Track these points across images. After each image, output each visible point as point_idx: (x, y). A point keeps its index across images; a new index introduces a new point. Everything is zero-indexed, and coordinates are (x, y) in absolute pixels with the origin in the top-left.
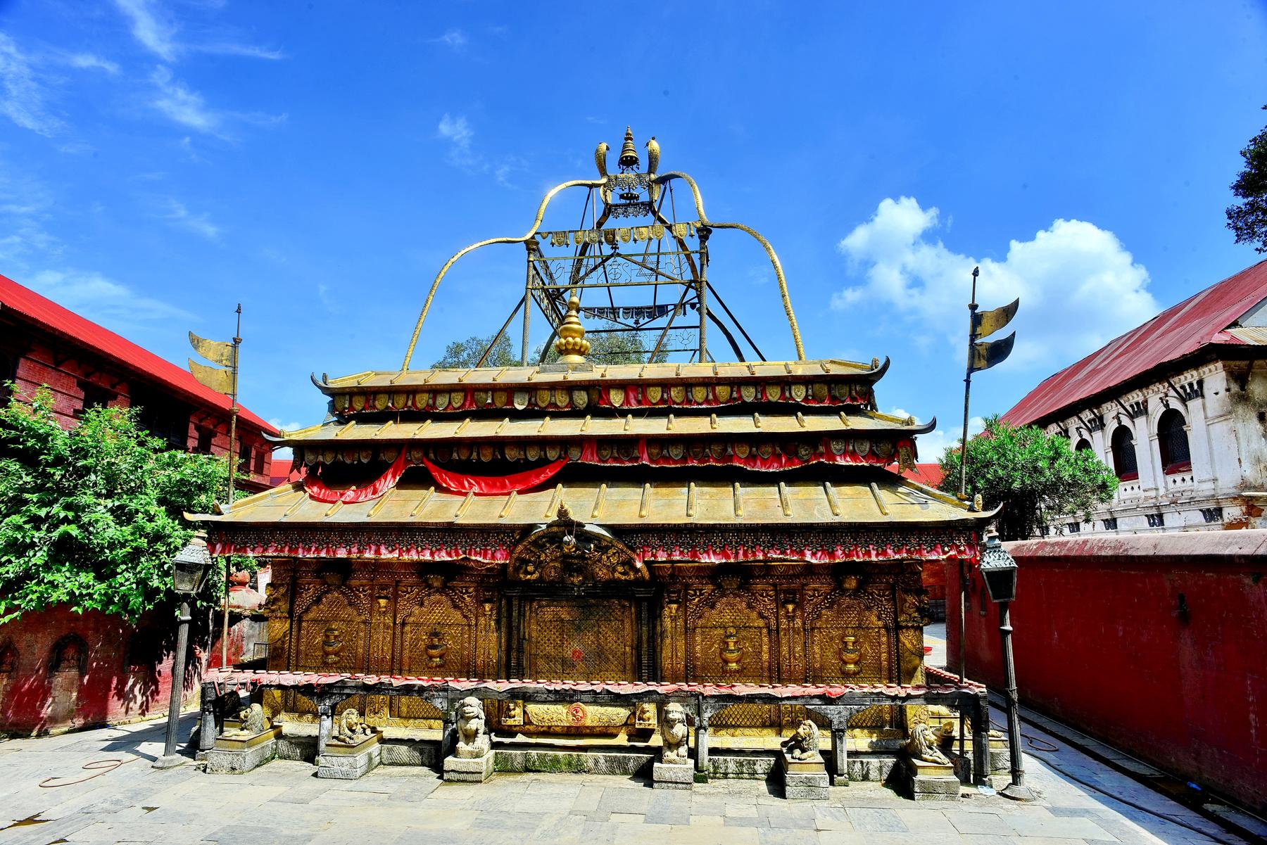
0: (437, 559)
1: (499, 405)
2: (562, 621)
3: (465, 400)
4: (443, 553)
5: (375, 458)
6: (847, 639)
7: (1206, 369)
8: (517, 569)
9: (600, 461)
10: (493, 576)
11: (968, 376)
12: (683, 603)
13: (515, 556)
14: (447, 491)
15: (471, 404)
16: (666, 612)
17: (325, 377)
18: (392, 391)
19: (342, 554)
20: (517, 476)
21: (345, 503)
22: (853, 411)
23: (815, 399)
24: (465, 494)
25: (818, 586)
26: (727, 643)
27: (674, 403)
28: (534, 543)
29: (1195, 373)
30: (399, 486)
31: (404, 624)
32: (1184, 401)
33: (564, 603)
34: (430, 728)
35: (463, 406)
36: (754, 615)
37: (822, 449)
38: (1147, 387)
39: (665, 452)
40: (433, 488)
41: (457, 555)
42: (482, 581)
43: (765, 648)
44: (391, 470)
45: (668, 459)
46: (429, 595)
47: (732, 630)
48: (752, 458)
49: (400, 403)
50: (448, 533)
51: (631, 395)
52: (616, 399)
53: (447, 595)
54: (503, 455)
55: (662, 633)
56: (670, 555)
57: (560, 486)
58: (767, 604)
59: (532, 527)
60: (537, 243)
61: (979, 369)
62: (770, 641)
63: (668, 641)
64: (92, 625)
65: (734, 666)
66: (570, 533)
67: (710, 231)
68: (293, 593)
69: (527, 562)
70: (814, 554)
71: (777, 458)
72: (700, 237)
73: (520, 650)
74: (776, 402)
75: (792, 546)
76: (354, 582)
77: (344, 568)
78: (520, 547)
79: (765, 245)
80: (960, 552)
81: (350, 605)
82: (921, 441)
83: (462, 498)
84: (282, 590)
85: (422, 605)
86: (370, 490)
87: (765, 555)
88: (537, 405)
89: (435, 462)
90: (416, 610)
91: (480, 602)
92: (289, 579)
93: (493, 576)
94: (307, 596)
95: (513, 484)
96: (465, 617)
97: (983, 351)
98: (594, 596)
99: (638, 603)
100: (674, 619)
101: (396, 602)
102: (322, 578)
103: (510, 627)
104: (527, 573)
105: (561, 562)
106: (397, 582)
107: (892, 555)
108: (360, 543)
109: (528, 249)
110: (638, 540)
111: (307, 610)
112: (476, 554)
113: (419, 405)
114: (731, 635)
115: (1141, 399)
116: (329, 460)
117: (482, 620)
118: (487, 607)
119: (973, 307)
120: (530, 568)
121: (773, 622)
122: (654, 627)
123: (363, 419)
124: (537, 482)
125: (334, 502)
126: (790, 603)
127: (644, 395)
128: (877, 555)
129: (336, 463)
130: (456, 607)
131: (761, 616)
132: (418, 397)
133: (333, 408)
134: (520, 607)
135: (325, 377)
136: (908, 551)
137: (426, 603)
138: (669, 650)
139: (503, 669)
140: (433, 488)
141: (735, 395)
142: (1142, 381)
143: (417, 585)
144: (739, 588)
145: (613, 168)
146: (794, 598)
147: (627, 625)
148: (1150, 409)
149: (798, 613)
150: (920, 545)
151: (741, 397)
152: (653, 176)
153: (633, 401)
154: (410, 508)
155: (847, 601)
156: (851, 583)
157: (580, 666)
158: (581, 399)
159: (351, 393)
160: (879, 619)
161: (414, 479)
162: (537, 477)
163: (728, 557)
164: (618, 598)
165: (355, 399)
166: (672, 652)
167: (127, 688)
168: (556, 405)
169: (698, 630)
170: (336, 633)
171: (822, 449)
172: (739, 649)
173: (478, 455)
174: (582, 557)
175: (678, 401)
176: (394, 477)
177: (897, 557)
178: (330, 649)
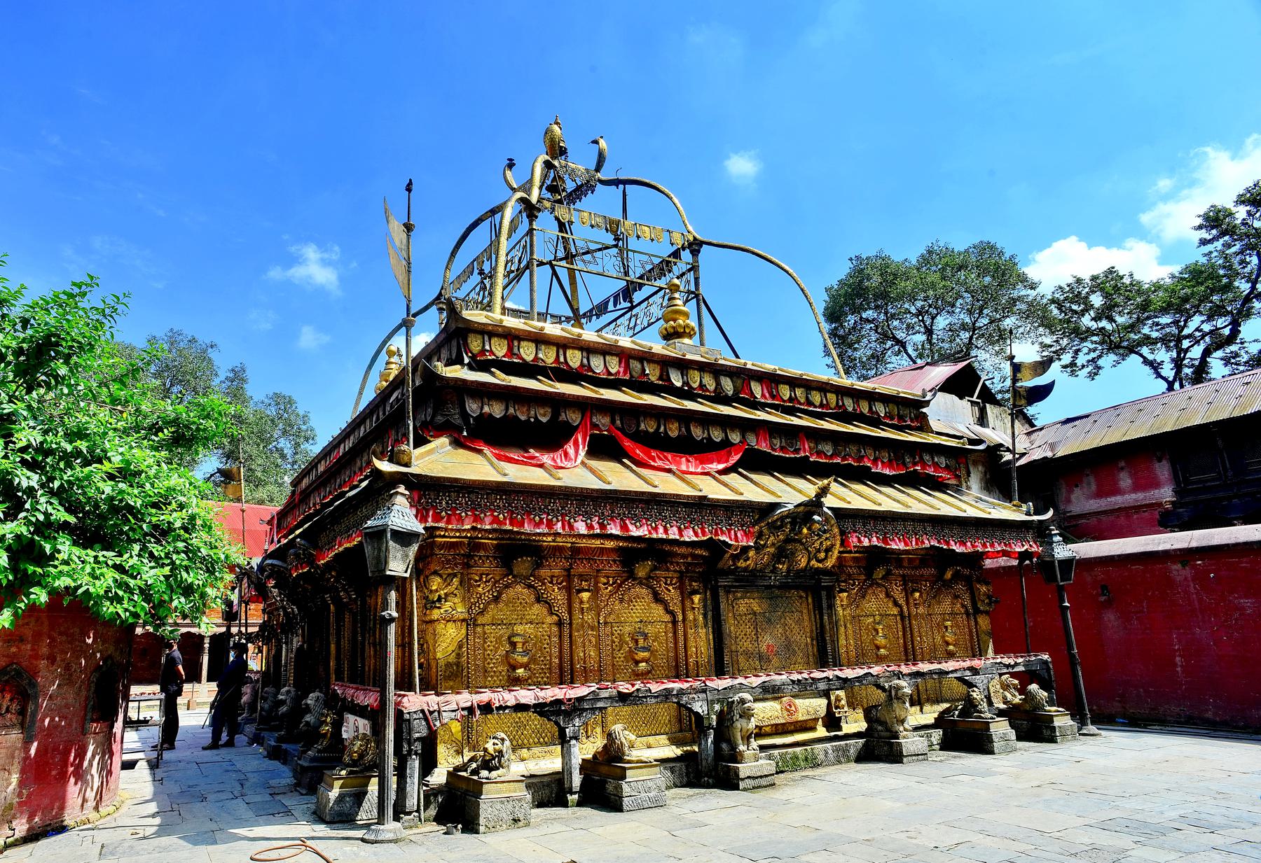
2: (755, 614)
5: (555, 415)
34: (649, 747)
35: (618, 372)
41: (704, 534)
42: (687, 571)
45: (820, 454)
49: (548, 356)
50: (700, 507)
54: (688, 430)
55: (837, 622)
63: (842, 629)
64: (45, 650)
76: (544, 572)
81: (538, 600)
89: (622, 430)
98: (779, 588)
106: (598, 571)
108: (602, 516)
112: (723, 533)
116: (497, 410)
121: (905, 608)
131: (896, 604)
157: (775, 661)
158: (728, 385)
161: (603, 449)
166: (845, 642)
167: (86, 764)
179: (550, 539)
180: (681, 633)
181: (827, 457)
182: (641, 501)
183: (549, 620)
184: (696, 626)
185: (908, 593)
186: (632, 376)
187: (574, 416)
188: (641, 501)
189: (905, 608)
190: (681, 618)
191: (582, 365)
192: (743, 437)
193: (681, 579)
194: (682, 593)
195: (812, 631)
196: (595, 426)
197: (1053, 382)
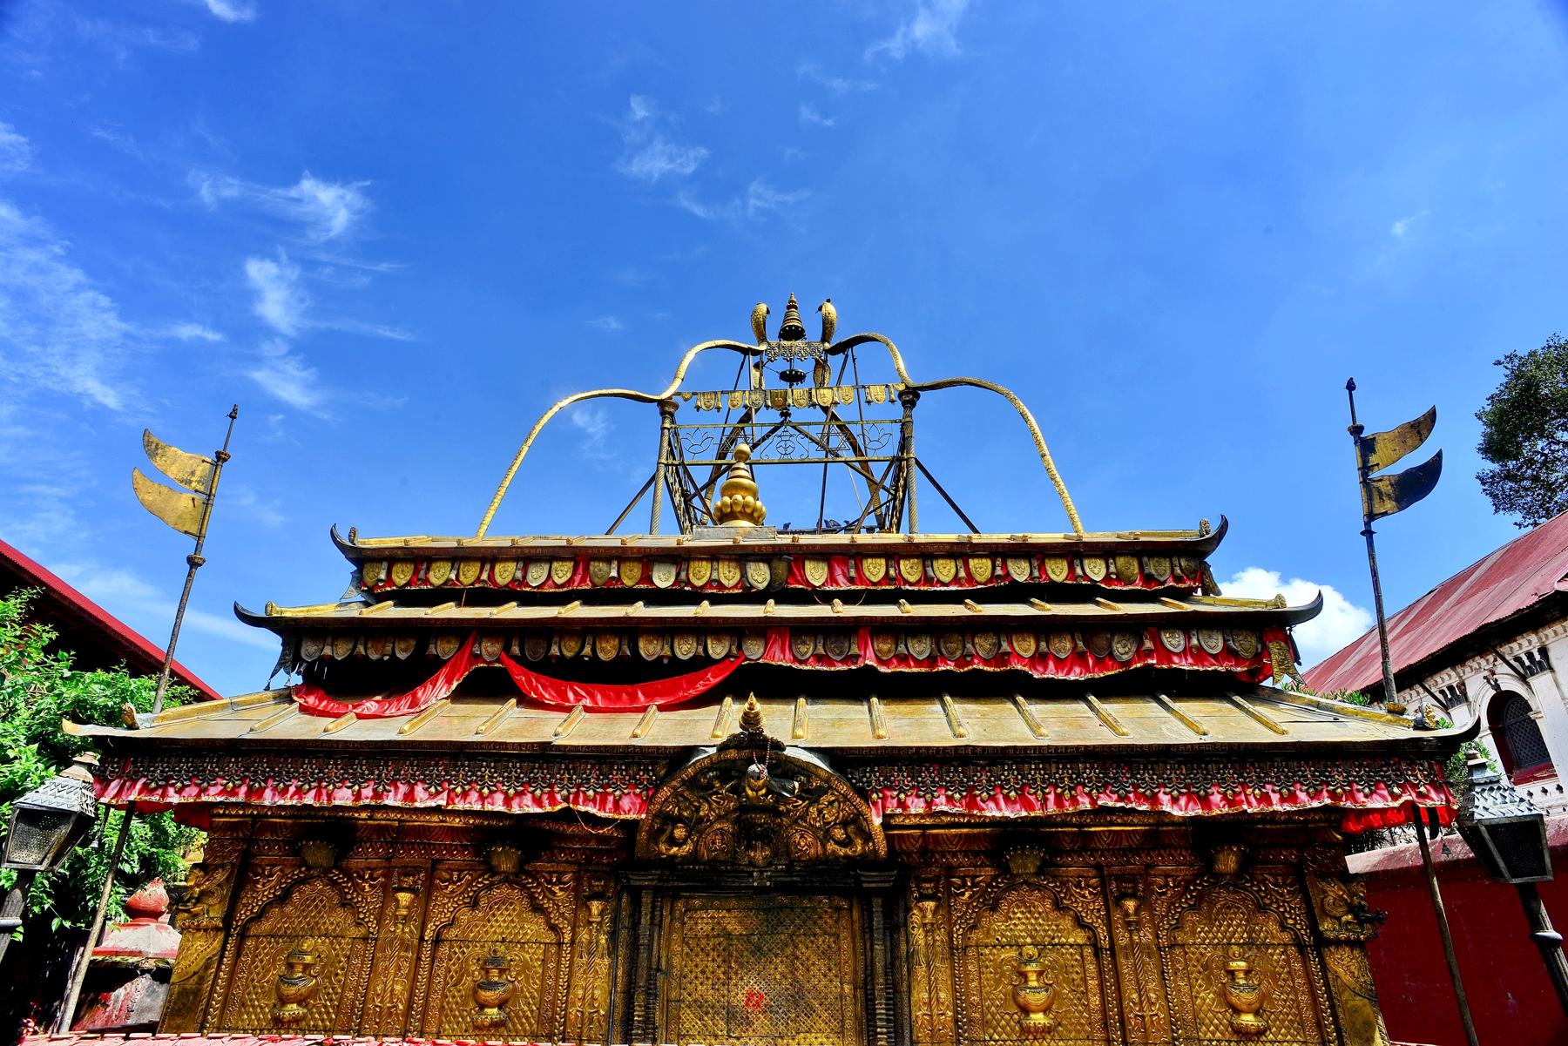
0: (516, 810)
1: (628, 582)
2: (728, 935)
3: (574, 573)
4: (528, 799)
5: (421, 648)
6: (1234, 965)
7: (1549, 631)
8: (654, 836)
9: (796, 660)
10: (608, 853)
11: (1367, 524)
12: (944, 901)
13: (654, 808)
14: (538, 704)
15: (583, 581)
16: (916, 917)
17: (353, 533)
18: (457, 556)
19: (343, 797)
20: (658, 684)
21: (360, 717)
22: (1185, 595)
23: (1119, 580)
24: (569, 710)
25: (1170, 867)
26: (1024, 975)
27: (906, 582)
28: (692, 783)
29: (1533, 637)
30: (457, 697)
31: (438, 941)
32: (1523, 679)
33: (733, 903)
35: (570, 581)
36: (1067, 923)
37: (1148, 644)
38: (1462, 662)
39: (902, 648)
40: (513, 701)
41: (553, 802)
42: (588, 861)
43: (1093, 983)
44: (445, 671)
45: (904, 659)
46: (489, 887)
47: (1031, 950)
48: (1040, 659)
49: (469, 575)
50: (542, 760)
51: (838, 572)
52: (816, 574)
53: (523, 887)
54: (635, 649)
55: (910, 956)
56: (929, 804)
57: (728, 700)
58: (1088, 903)
59: (690, 751)
60: (676, 406)
61: (1385, 514)
62: (1100, 972)
63: (921, 971)
65: (1038, 1019)
66: (761, 761)
67: (918, 396)
68: (241, 881)
69: (675, 820)
70: (1175, 801)
71: (1078, 658)
72: (904, 404)
73: (651, 993)
74: (1062, 584)
75: (1136, 787)
76: (356, 862)
77: (337, 832)
78: (666, 791)
79: (1007, 396)
80: (1420, 795)
81: (343, 905)
82: (1300, 633)
83: (564, 715)
84: (220, 876)
85: (474, 904)
86: (405, 702)
87: (1093, 802)
88: (689, 583)
89: (521, 660)
90: (465, 916)
91: (582, 901)
92: (243, 847)
93: (608, 853)
94: (265, 890)
95: (650, 696)
96: (553, 928)
97: (1385, 487)
99: (864, 898)
100: (929, 929)
101: (428, 899)
102: (296, 852)
103: (634, 946)
104: (672, 841)
105: (737, 821)
106: (435, 862)
107: (1306, 801)
109: (663, 413)
110: (874, 777)
111: (259, 917)
112: (587, 800)
113: (499, 580)
114: (1030, 960)
115: (1454, 681)
116: (340, 652)
117: (584, 936)
118: (596, 907)
119: (1356, 430)
120: (679, 832)
121: (1102, 933)
122: (894, 947)
123: (403, 598)
124: (692, 692)
125: (338, 716)
126: (1133, 896)
127: (859, 569)
128: (1282, 800)
129: (352, 658)
130: (537, 908)
131: (1079, 923)
132: (498, 568)
133: (359, 580)
134: (654, 908)
135: (353, 534)
136: (1332, 795)
137: (483, 902)
138: (924, 985)
139: (618, 1028)
140: (513, 701)
141: (999, 572)
142: (1455, 654)
143: (471, 868)
144: (1040, 871)
145: (773, 331)
146: (1135, 889)
147: (845, 945)
148: (1470, 694)
149: (1145, 915)
150: (1350, 784)
151: (1008, 574)
152: (827, 345)
153: (841, 579)
154: (476, 724)
155: (1223, 896)
156: (1228, 862)
159: (391, 558)
160: (1283, 928)
162: (692, 685)
163: (1029, 806)
164: (829, 892)
165: (397, 568)
168: (721, 586)
169: (971, 953)
170: (308, 959)
171: (1148, 644)
172: (1047, 987)
173: (594, 650)
174: (773, 811)
175: (912, 579)
176: (449, 682)
177: (1315, 804)
178: (293, 990)
179: (364, 815)
180: (565, 963)
181: (918, 663)
182: (416, 755)
183: (355, 932)
184: (590, 954)
185: (1112, 902)
186: (594, 585)
187: (447, 647)
188: (488, 756)
189: (1102, 933)
190: (567, 938)
191: (514, 580)
192: (739, 648)
193: (577, 879)
194: (576, 897)
195: (855, 972)
196: (479, 658)
197: (1439, 455)
